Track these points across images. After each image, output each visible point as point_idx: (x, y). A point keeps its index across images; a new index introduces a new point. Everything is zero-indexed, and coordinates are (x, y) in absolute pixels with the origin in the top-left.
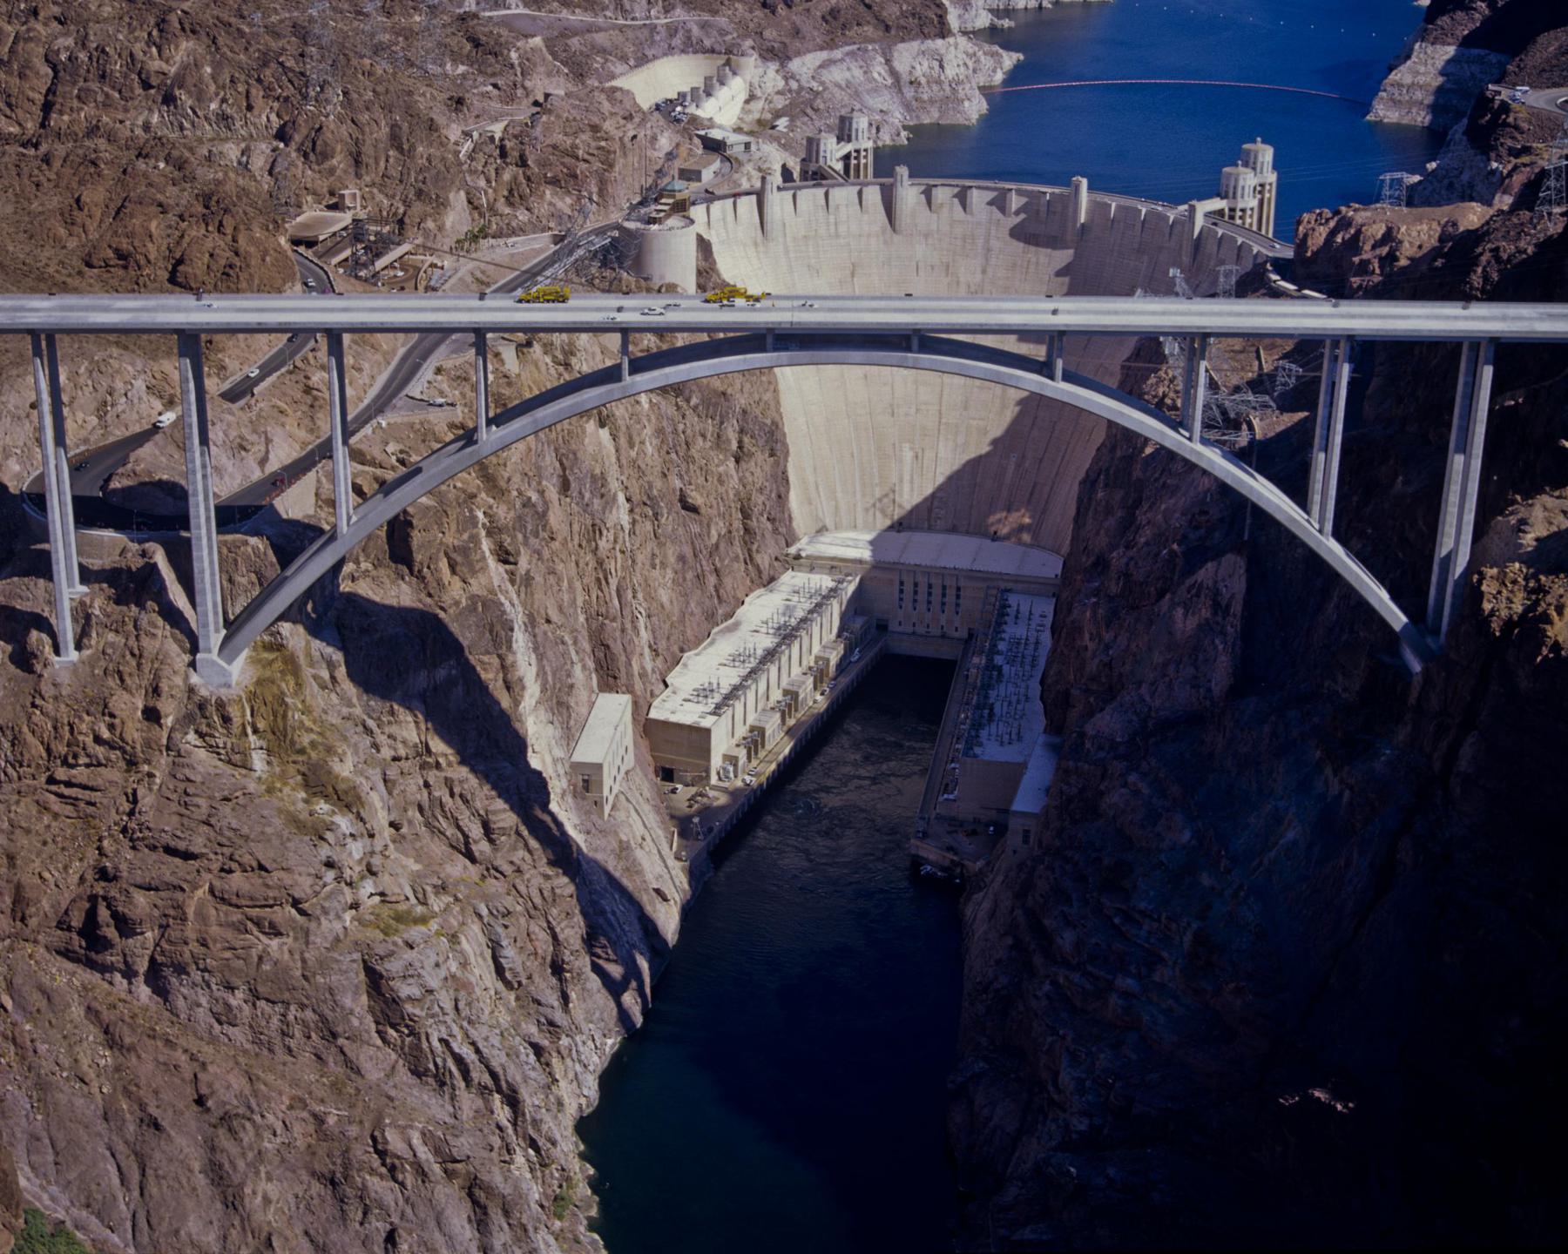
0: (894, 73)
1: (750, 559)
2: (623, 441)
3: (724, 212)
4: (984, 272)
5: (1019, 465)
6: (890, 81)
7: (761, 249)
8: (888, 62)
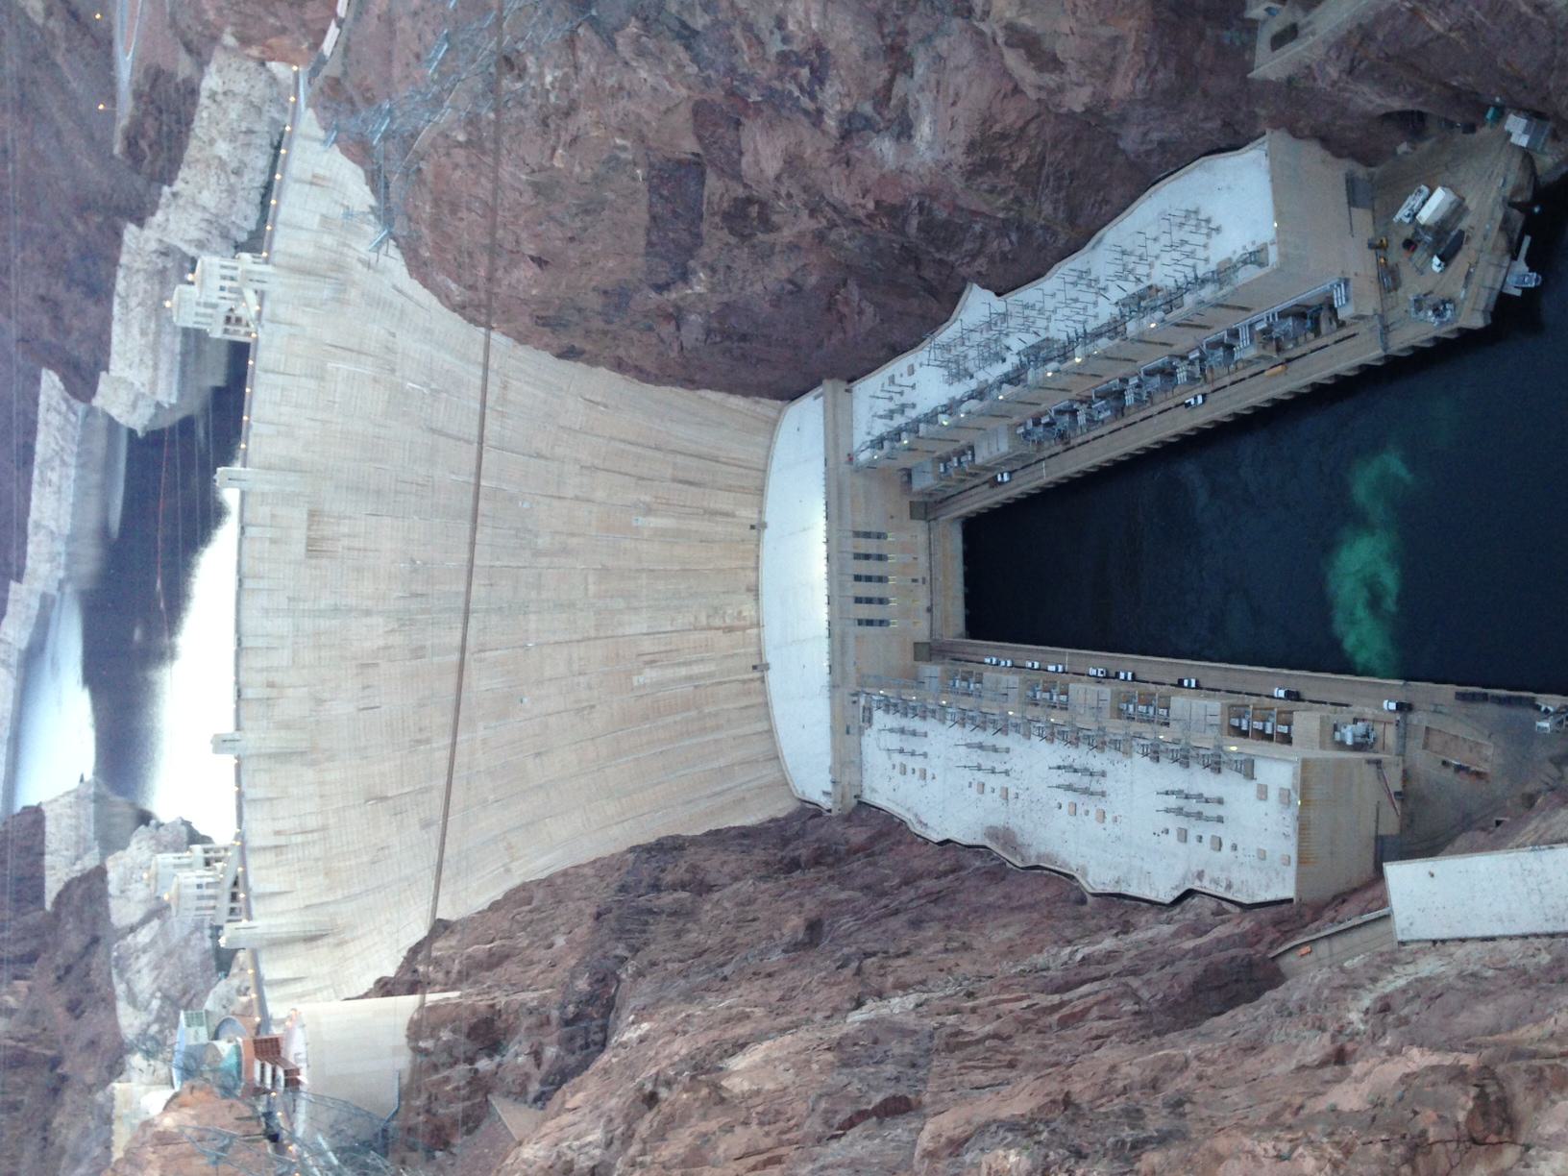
0: (145, 921)
1: (866, 850)
2: (742, 1030)
3: (282, 1000)
4: (368, 613)
5: (649, 511)
6: (155, 923)
7: (347, 936)
8: (132, 929)
